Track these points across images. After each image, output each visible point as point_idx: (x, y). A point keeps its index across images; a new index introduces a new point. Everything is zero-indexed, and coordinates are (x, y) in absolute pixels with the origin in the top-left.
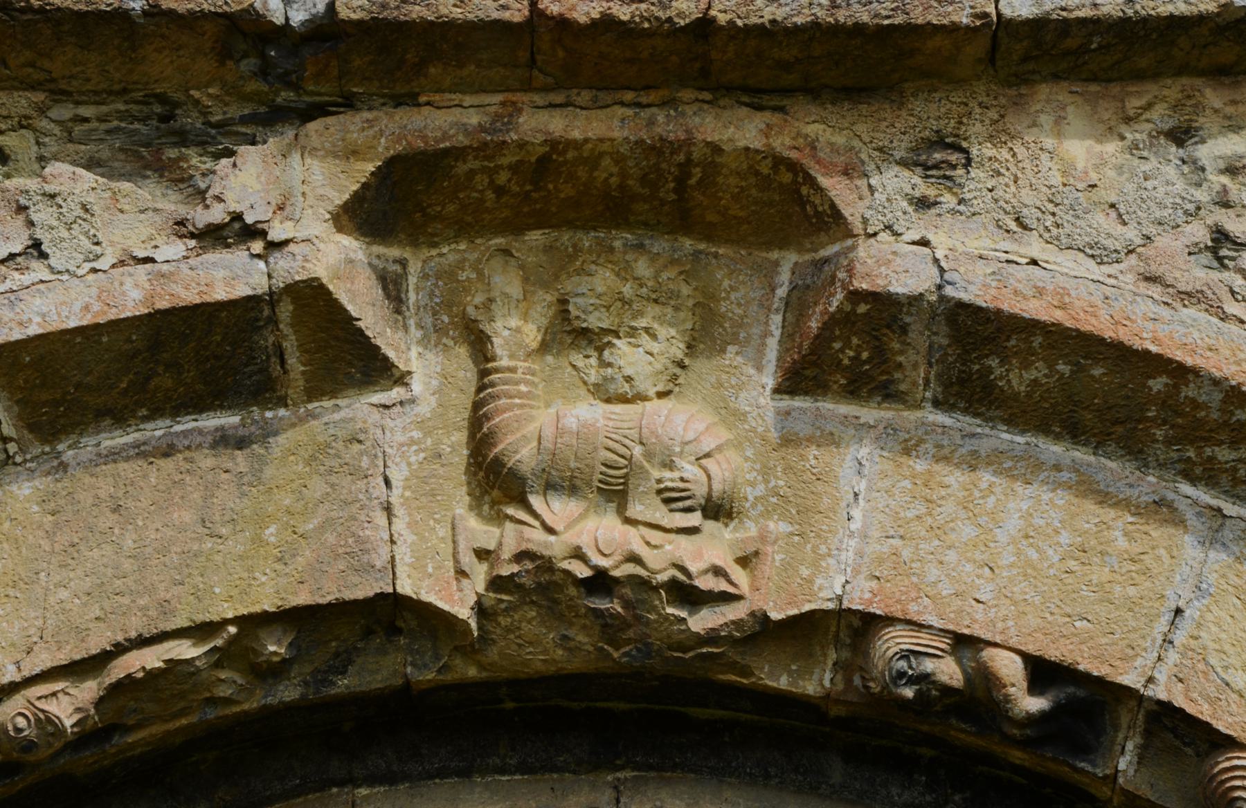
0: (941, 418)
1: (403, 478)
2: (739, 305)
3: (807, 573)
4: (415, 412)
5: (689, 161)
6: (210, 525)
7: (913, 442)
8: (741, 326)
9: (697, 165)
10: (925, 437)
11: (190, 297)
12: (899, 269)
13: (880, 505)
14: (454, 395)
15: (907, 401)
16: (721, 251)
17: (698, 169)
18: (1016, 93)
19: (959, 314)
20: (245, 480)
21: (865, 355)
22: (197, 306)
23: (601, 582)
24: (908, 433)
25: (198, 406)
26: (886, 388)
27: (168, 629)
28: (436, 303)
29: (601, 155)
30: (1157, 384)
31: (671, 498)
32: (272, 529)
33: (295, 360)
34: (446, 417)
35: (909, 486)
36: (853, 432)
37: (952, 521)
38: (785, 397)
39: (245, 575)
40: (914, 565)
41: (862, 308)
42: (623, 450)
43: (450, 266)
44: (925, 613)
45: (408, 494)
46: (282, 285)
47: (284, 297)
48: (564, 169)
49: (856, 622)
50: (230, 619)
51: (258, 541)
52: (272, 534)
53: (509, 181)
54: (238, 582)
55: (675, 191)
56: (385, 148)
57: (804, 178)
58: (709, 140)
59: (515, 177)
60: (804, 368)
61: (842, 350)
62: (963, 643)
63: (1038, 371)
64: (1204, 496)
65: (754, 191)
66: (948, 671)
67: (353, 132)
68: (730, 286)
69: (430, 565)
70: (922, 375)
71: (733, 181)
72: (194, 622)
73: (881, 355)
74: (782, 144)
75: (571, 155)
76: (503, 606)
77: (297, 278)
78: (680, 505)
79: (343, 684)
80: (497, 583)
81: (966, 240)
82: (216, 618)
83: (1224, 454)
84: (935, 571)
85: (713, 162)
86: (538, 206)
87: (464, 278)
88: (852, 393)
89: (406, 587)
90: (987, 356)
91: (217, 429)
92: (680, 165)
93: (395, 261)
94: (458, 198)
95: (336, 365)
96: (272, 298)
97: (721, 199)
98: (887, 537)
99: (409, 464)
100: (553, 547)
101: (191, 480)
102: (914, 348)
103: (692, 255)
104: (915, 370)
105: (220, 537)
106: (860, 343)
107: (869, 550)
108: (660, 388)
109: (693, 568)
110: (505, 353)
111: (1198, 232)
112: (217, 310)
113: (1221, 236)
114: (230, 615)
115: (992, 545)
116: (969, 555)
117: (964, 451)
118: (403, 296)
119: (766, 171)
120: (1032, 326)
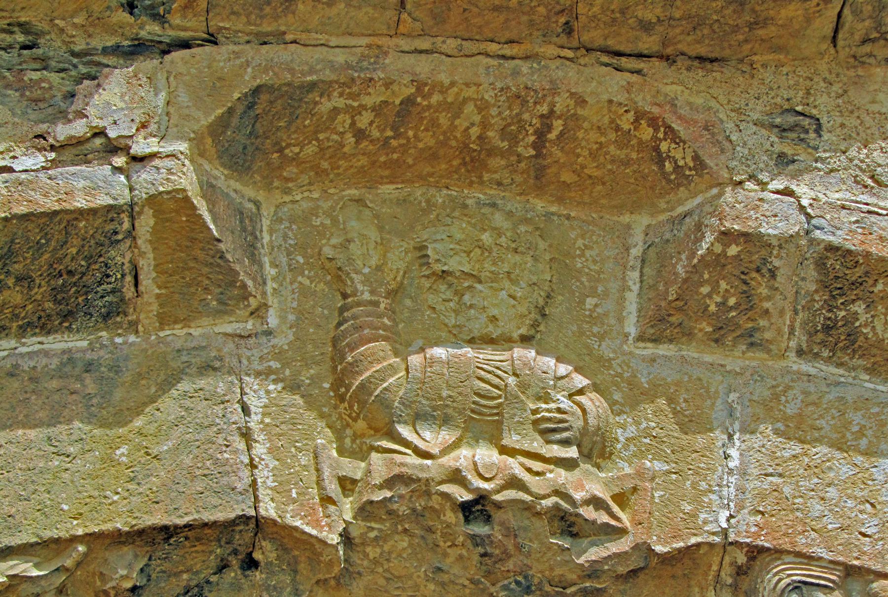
1: (262, 405)
2: (595, 262)
3: (690, 508)
4: (271, 344)
5: (552, 112)
6: (57, 444)
7: (781, 388)
8: (598, 280)
9: (559, 117)
10: (791, 384)
12: (768, 214)
13: (755, 445)
14: (311, 330)
15: (771, 350)
16: (573, 214)
17: (560, 122)
18: (854, 74)
19: (827, 258)
20: (95, 401)
21: (732, 301)
22: (56, 213)
24: (775, 380)
26: (751, 336)
27: (13, 544)
28: (290, 244)
29: (465, 101)
32: (123, 450)
33: (150, 281)
34: (303, 351)
35: (782, 428)
36: (721, 378)
37: (828, 461)
38: (649, 345)
39: (96, 493)
40: (796, 501)
41: (733, 250)
42: (496, 381)
43: (303, 212)
44: (813, 546)
45: (267, 420)
46: (144, 196)
47: (146, 209)
48: (427, 114)
49: (742, 559)
50: (80, 536)
51: (109, 460)
52: (123, 454)
53: (371, 123)
54: (88, 500)
55: (534, 146)
56: (249, 80)
57: (665, 133)
58: (573, 91)
59: (377, 120)
60: (669, 315)
61: (709, 296)
65: (612, 148)
67: (219, 61)
68: (585, 245)
69: (294, 491)
70: (788, 322)
71: (593, 136)
72: (41, 538)
75: (435, 98)
76: (372, 535)
77: (161, 189)
78: (558, 436)
80: (365, 511)
81: (827, 192)
82: (64, 534)
84: (818, 507)
85: (575, 114)
86: (395, 156)
87: (318, 223)
88: (716, 341)
89: (269, 509)
90: (853, 301)
91: (64, 352)
92: (542, 116)
93: (250, 200)
94: (317, 140)
95: (193, 290)
97: (578, 156)
98: (766, 475)
99: (268, 392)
101: (36, 400)
102: (781, 294)
103: (545, 216)
104: (781, 317)
105: (68, 456)
106: (728, 287)
107: (750, 486)
108: (523, 331)
109: (578, 496)
110: (366, 288)
112: (76, 219)
114: (80, 532)
115: (870, 482)
116: (849, 491)
117: (831, 397)
118: (258, 233)
119: (626, 127)
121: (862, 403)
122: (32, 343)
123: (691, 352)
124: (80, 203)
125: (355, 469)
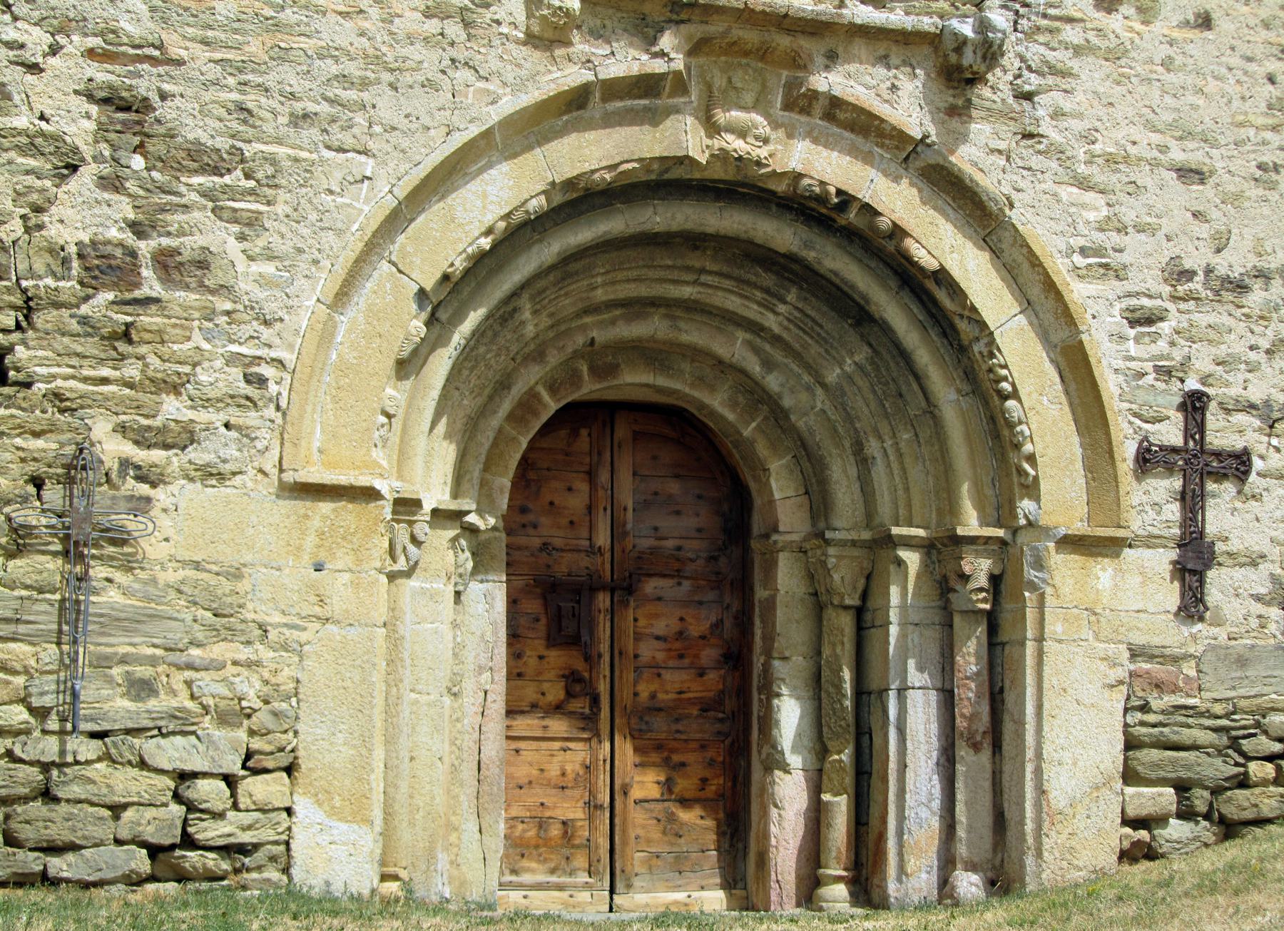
0: (820, 122)
11: (649, 71)
23: (740, 158)
25: (640, 97)
30: (876, 123)
31: (757, 138)
56: (699, 35)
62: (822, 183)
63: (848, 115)
64: (879, 150)
66: (817, 190)
73: (810, 105)
74: (795, 46)
79: (666, 176)
80: (712, 155)
83: (887, 142)
89: (691, 154)
96: (668, 73)
100: (729, 148)
111: (888, 84)
113: (894, 86)
120: (850, 104)
121: (833, 135)
122: (636, 102)
123: (792, 115)
124: (657, 71)
125: (709, 142)
